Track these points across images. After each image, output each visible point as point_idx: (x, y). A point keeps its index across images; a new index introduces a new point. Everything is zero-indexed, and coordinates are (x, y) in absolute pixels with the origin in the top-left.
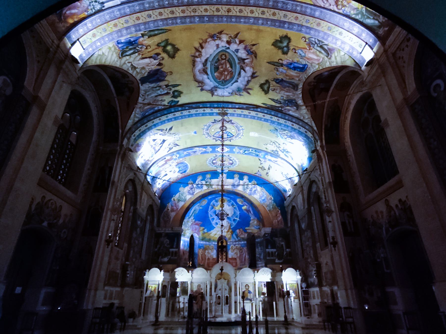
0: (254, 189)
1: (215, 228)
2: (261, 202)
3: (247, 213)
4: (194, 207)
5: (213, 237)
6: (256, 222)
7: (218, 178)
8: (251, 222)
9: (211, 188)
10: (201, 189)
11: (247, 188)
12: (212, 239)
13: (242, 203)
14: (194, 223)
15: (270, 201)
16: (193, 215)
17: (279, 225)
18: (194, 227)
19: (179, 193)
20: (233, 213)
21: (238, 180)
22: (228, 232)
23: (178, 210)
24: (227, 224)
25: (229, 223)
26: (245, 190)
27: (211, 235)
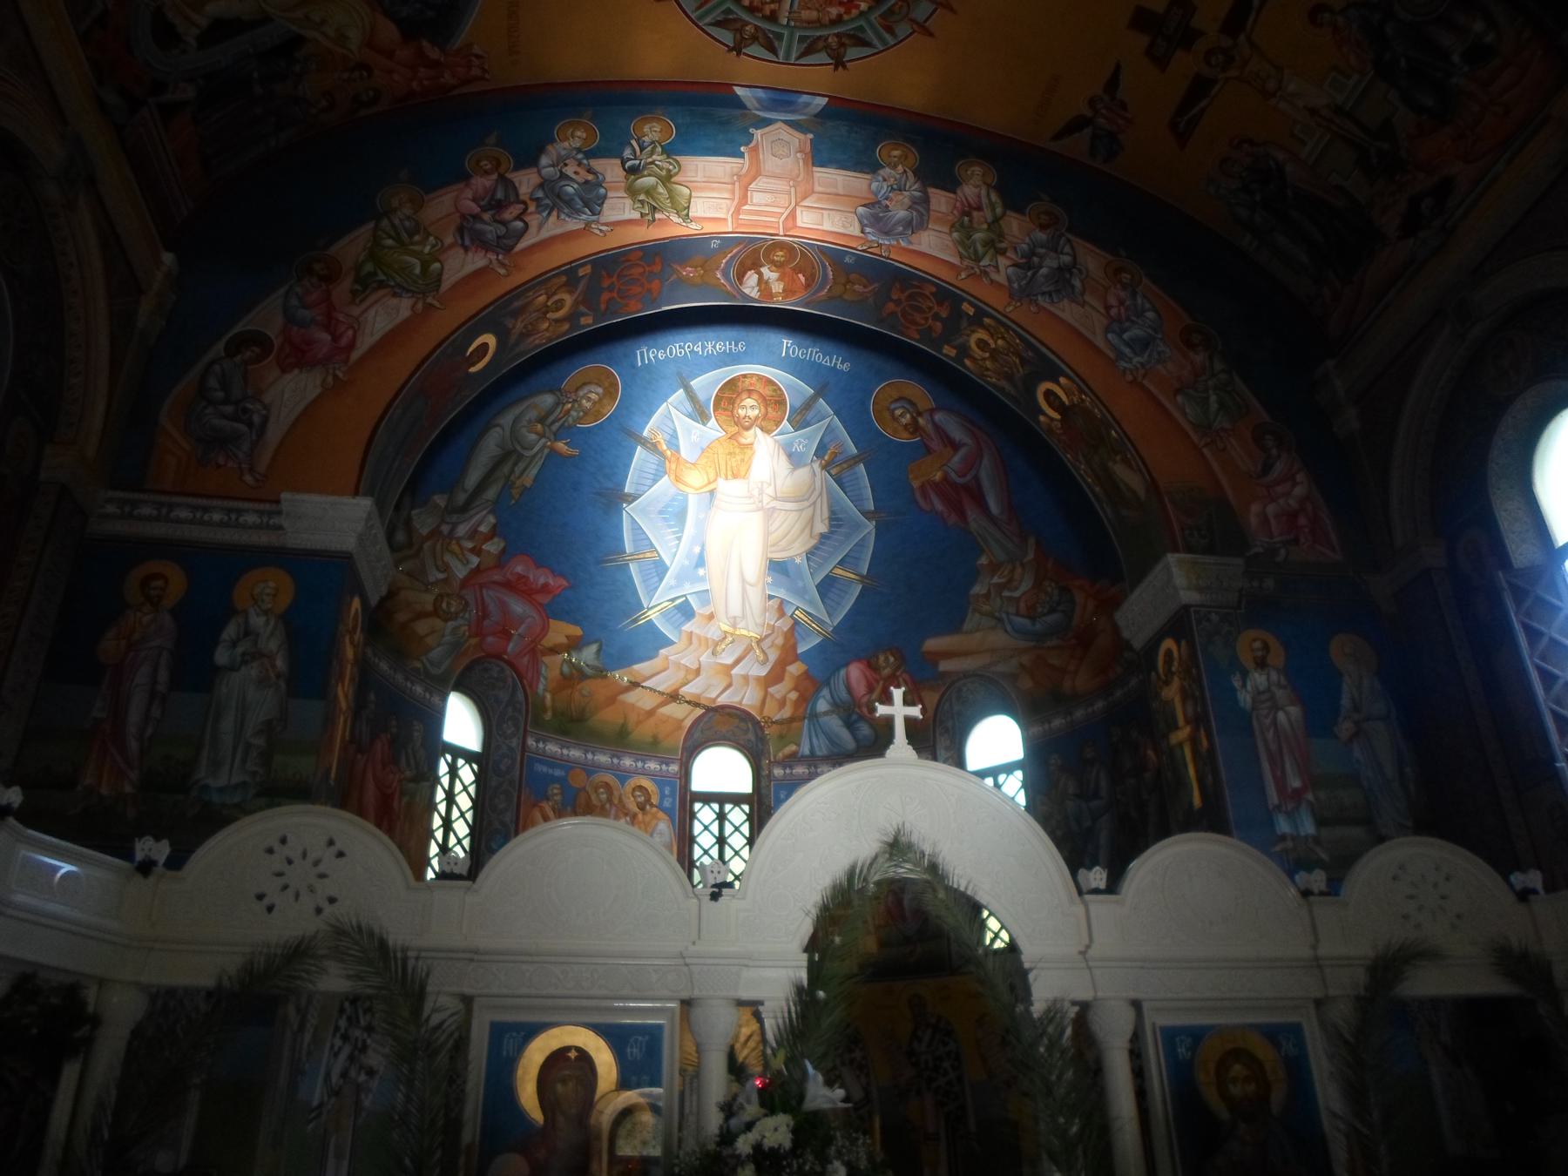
0: (1051, 262)
1: (672, 643)
2: (1121, 356)
3: (953, 519)
4: (507, 419)
5: (651, 713)
6: (1026, 585)
7: (741, 155)
8: (978, 589)
9: (675, 218)
10: (586, 216)
11: (989, 244)
12: (643, 732)
13: (914, 428)
14: (497, 577)
15: (1199, 358)
16: (491, 493)
17: (1296, 541)
18: (492, 607)
19: (364, 232)
20: (821, 527)
21: (913, 189)
22: (775, 676)
23: (355, 355)
24: (771, 618)
25: (781, 612)
26: (978, 259)
27: (632, 697)
